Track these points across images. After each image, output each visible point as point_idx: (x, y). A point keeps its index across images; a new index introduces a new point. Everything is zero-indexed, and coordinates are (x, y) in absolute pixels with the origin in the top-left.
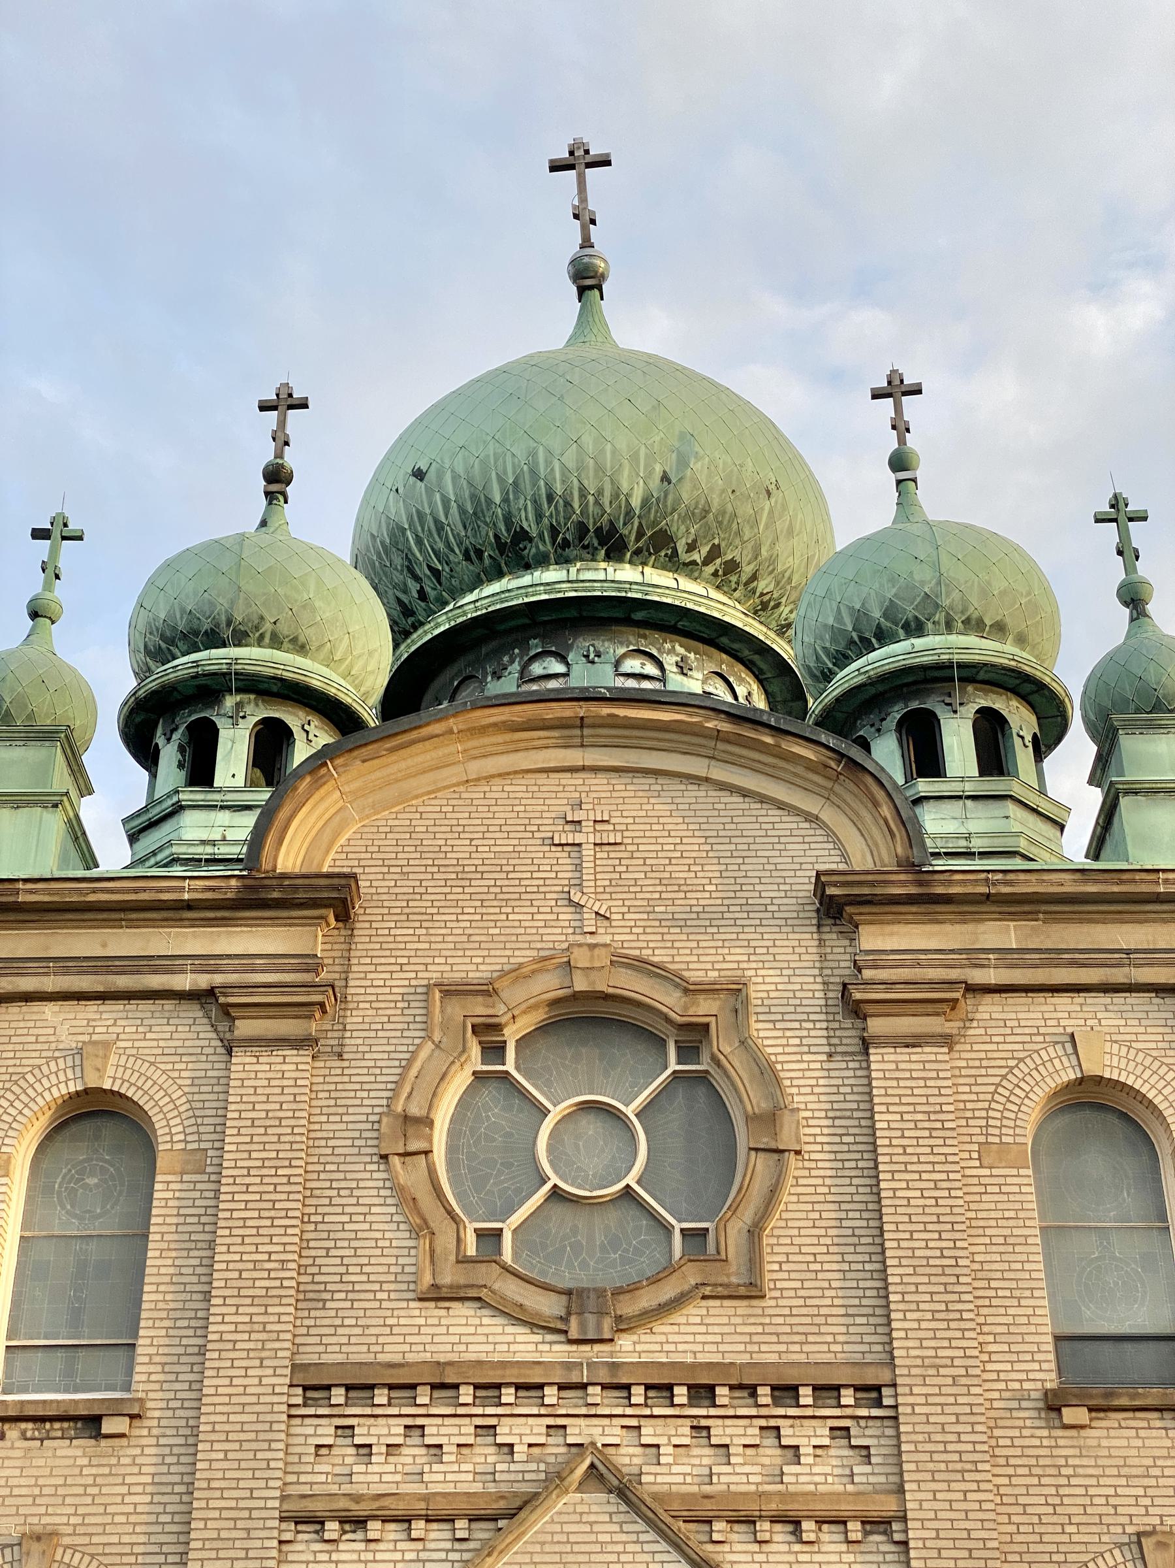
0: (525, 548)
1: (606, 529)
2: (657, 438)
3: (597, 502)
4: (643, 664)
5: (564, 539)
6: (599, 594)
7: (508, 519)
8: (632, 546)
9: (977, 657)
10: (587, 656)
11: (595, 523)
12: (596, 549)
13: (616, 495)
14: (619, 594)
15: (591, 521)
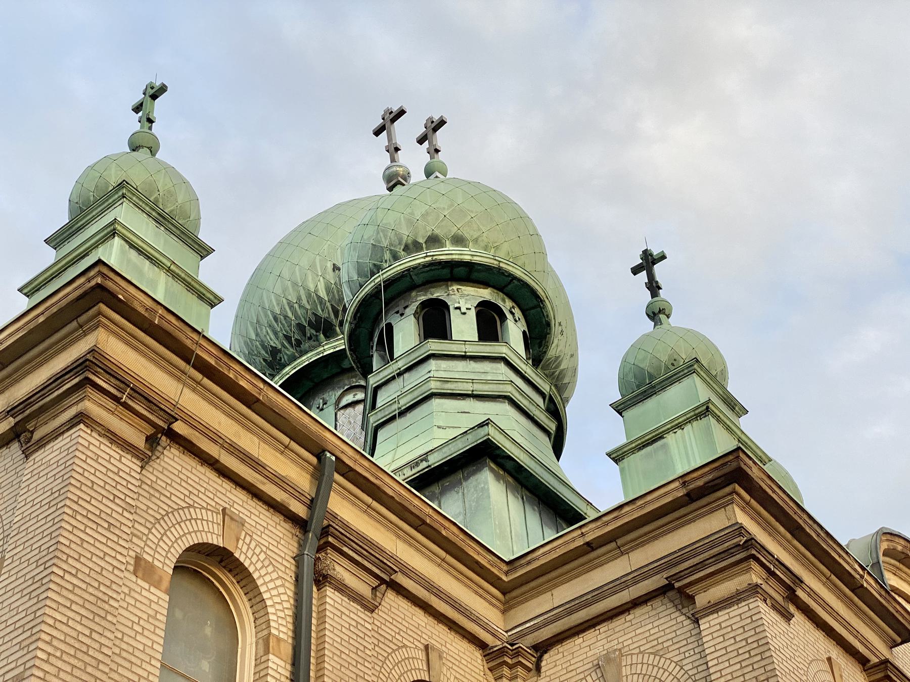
0: (281, 358)
1: (313, 320)
2: (326, 246)
3: (300, 306)
4: (356, 394)
5: (296, 340)
6: (307, 363)
7: (264, 347)
8: (336, 322)
9: (399, 268)
10: (318, 408)
11: (306, 321)
12: (317, 336)
13: (309, 296)
14: (318, 357)
15: (303, 319)
